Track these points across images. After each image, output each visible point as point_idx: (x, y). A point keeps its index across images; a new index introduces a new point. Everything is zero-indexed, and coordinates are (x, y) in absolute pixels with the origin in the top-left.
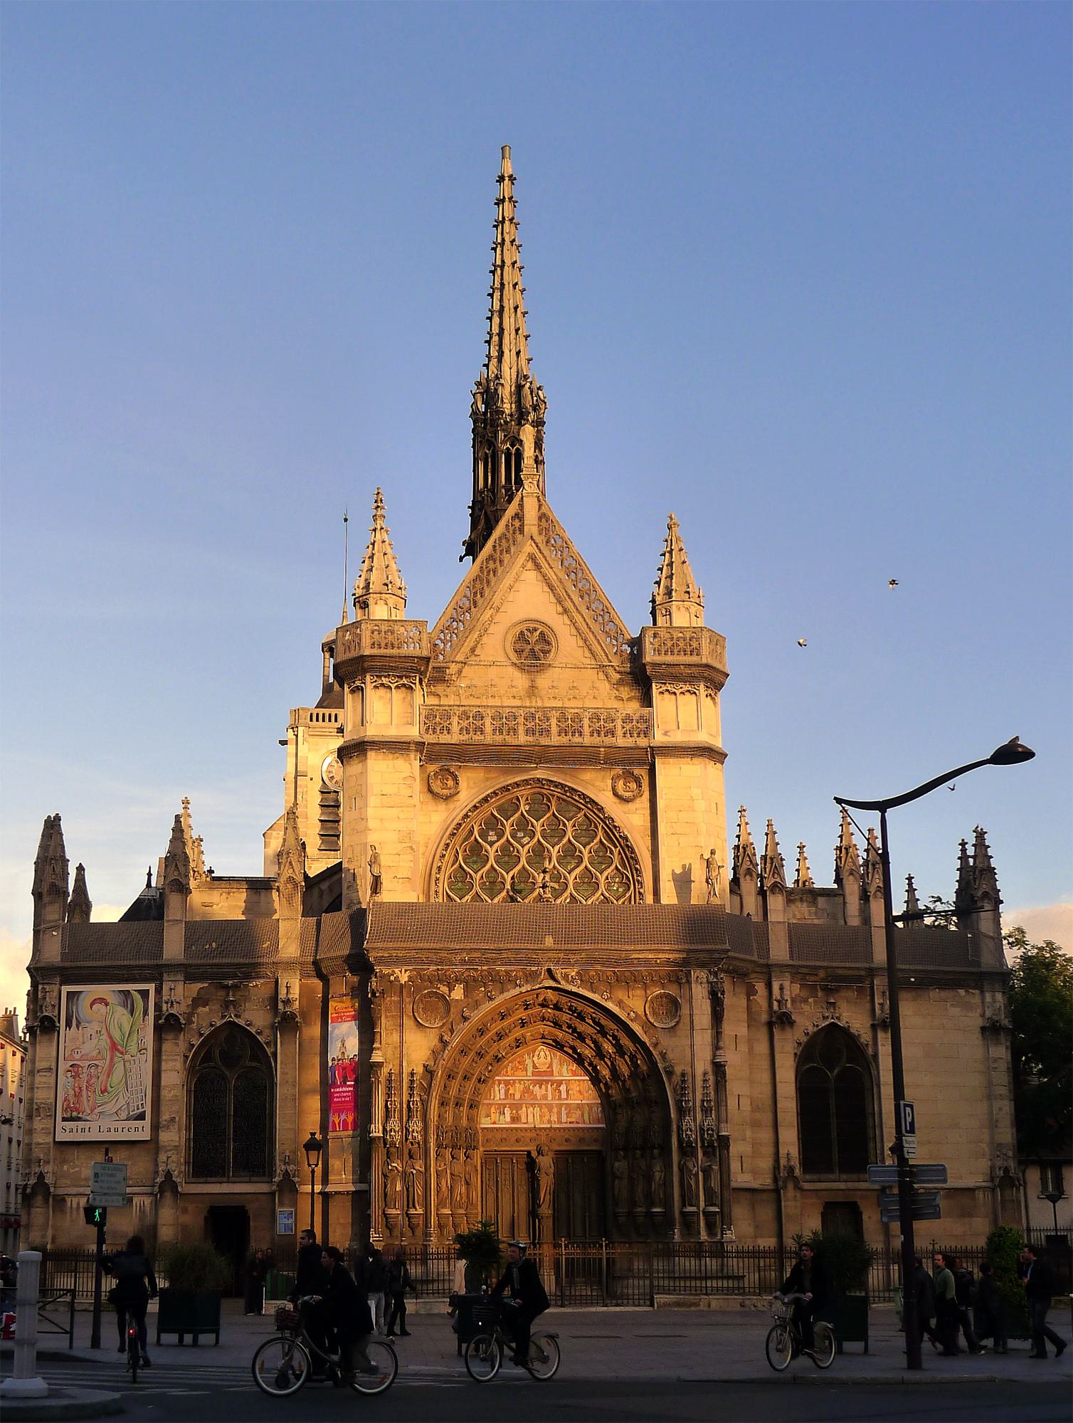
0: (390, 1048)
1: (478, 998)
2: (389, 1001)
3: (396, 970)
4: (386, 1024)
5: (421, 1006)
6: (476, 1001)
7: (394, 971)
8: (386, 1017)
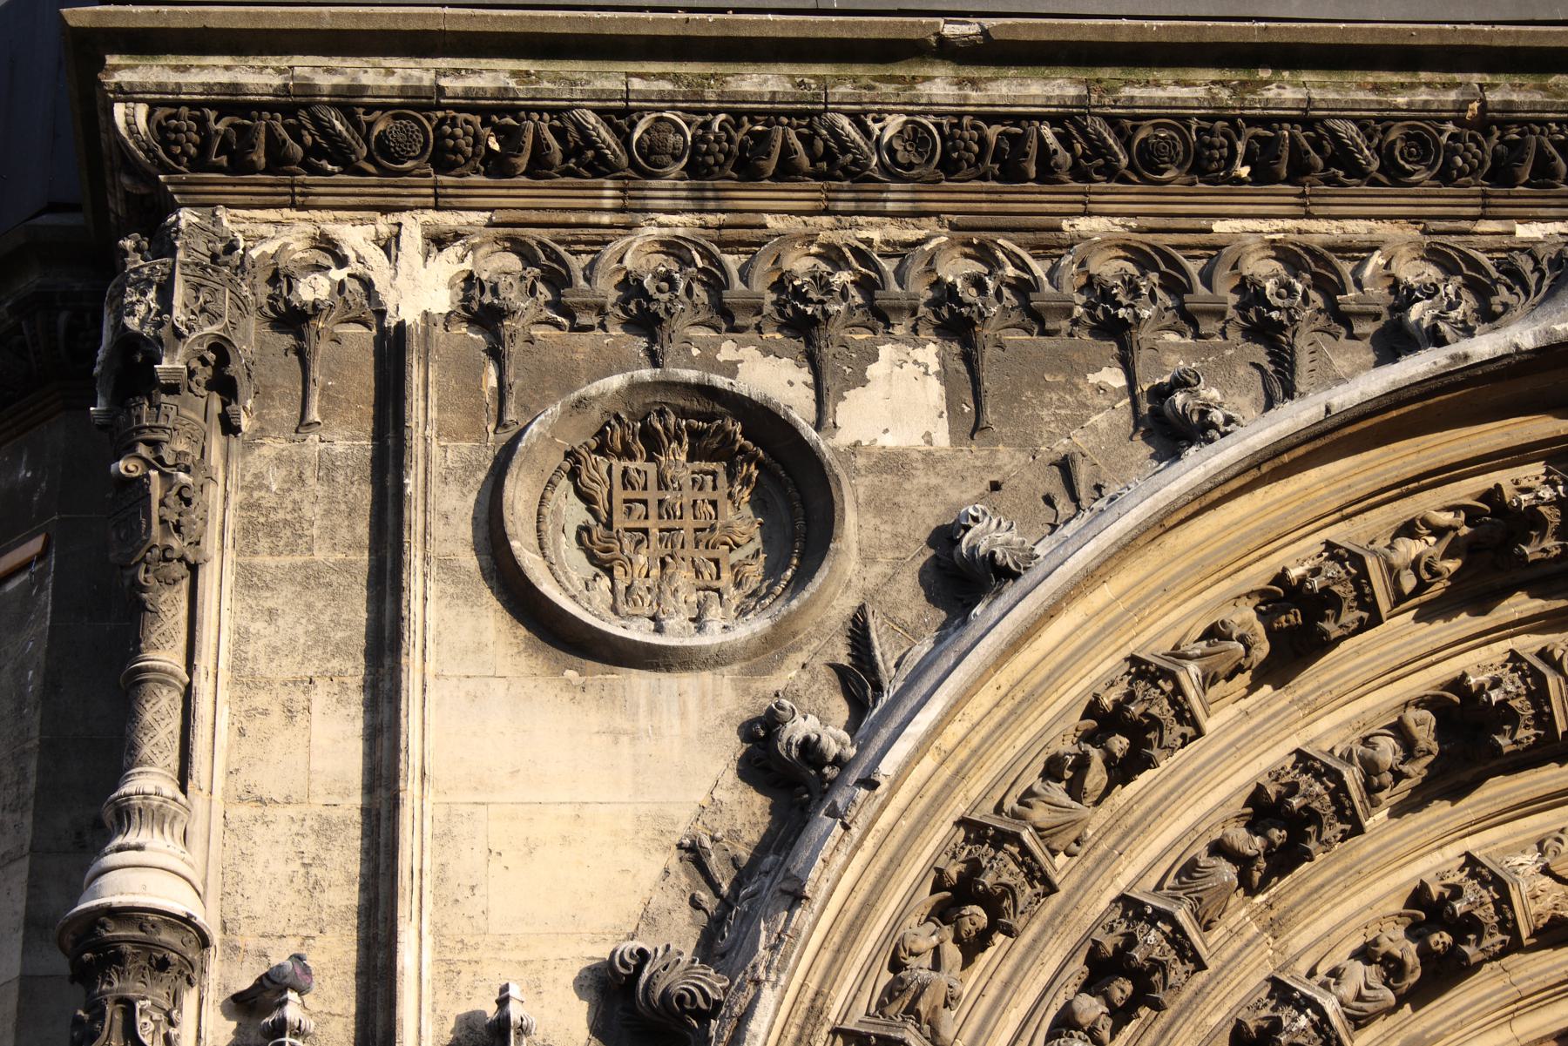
0: (282, 829)
1: (1079, 440)
2: (279, 460)
3: (355, 236)
4: (242, 636)
5: (574, 512)
6: (1065, 467)
7: (327, 245)
8: (249, 580)
